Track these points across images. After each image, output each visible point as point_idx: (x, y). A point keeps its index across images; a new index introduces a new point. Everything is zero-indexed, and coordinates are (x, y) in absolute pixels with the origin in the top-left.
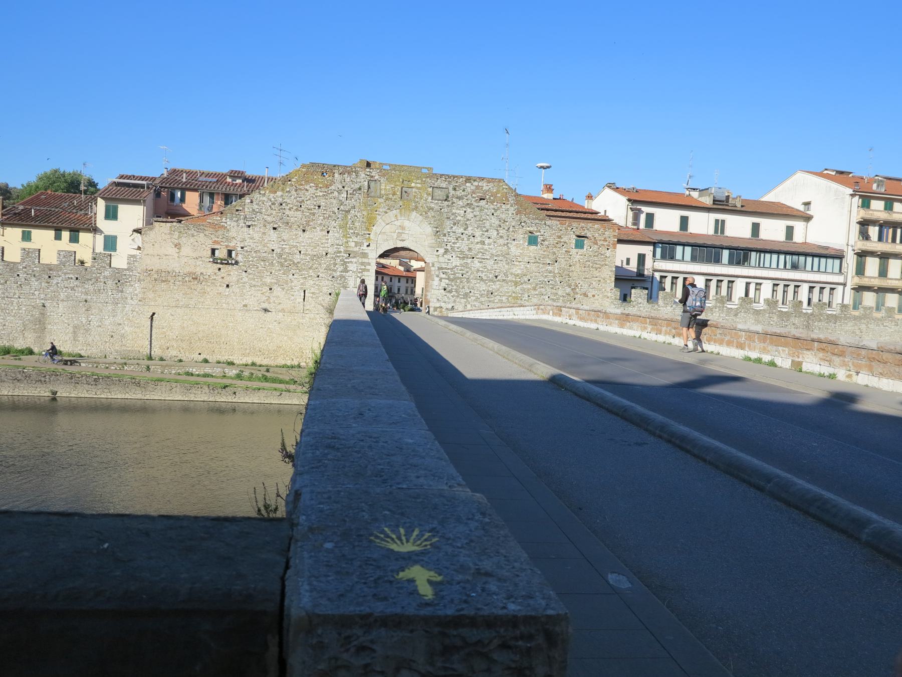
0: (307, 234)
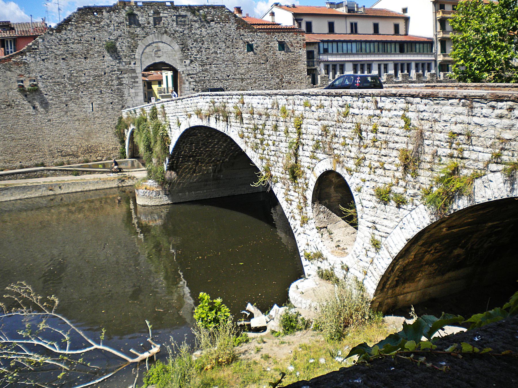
0: (88, 61)
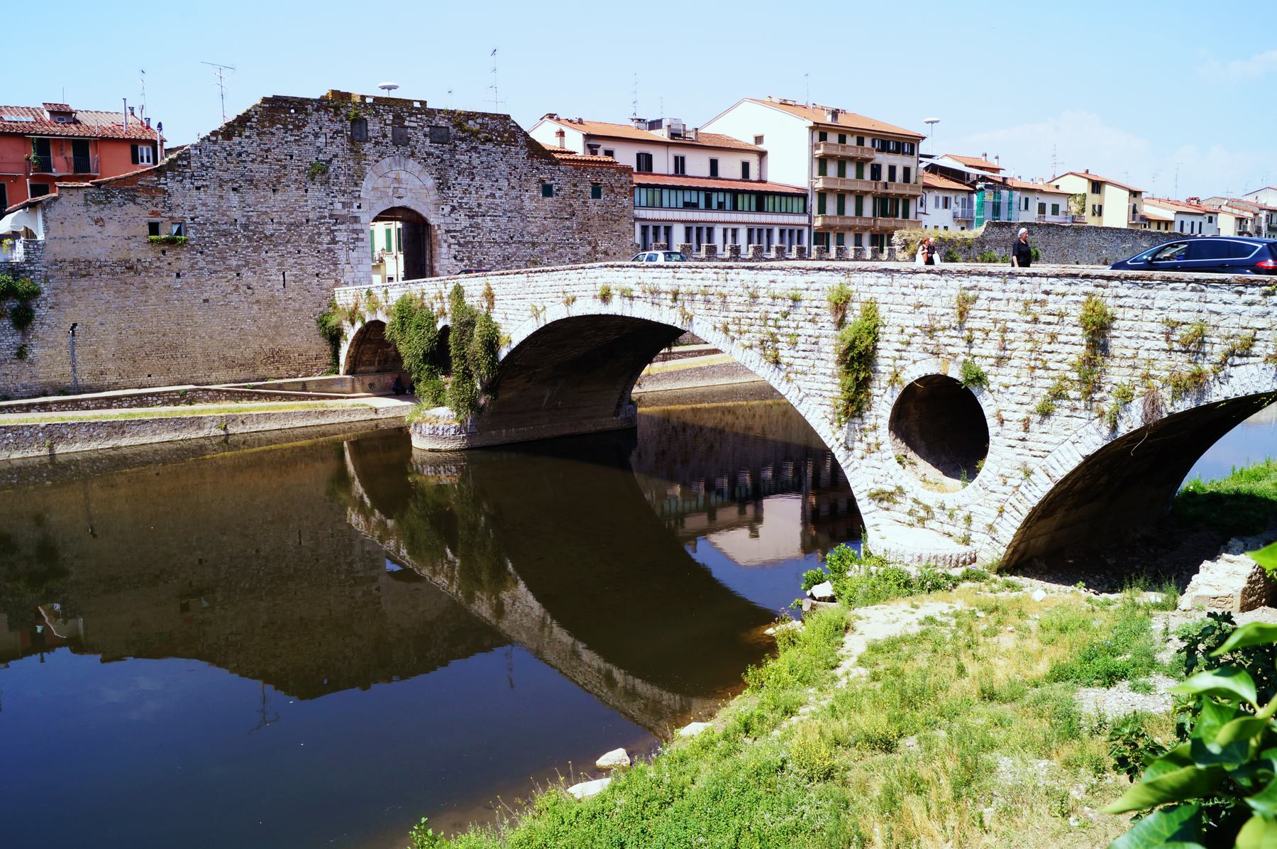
0: (279, 196)
